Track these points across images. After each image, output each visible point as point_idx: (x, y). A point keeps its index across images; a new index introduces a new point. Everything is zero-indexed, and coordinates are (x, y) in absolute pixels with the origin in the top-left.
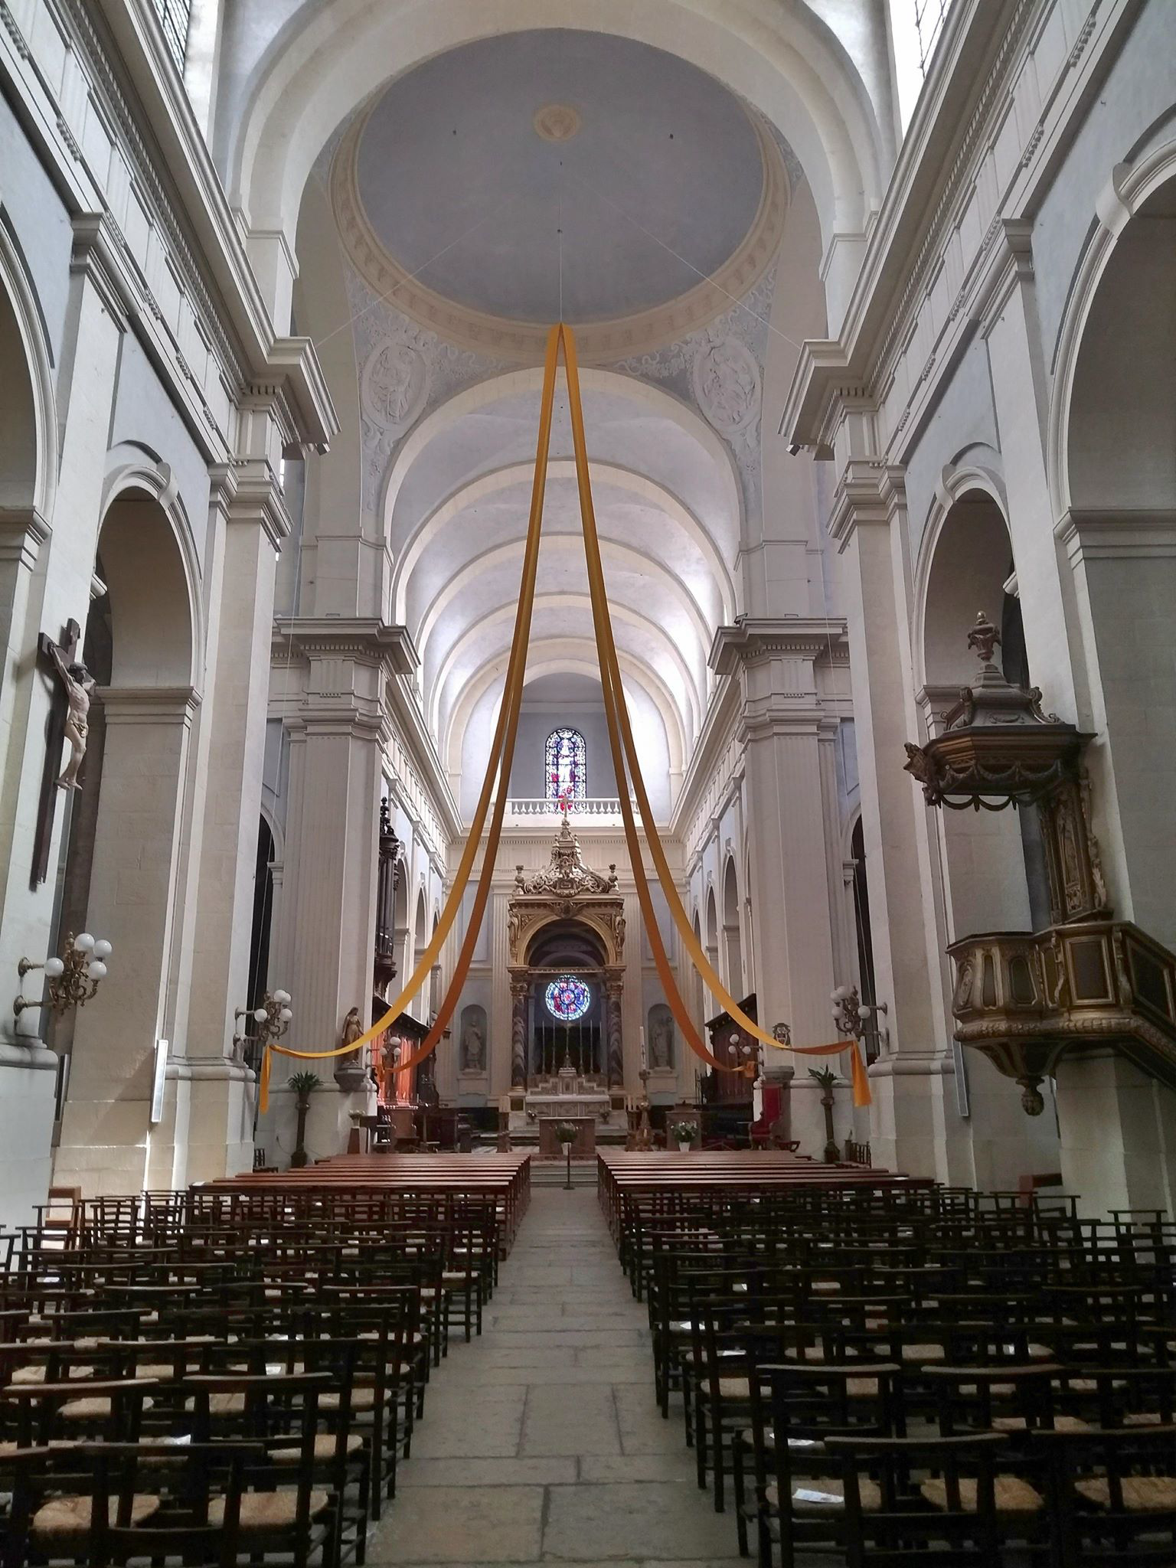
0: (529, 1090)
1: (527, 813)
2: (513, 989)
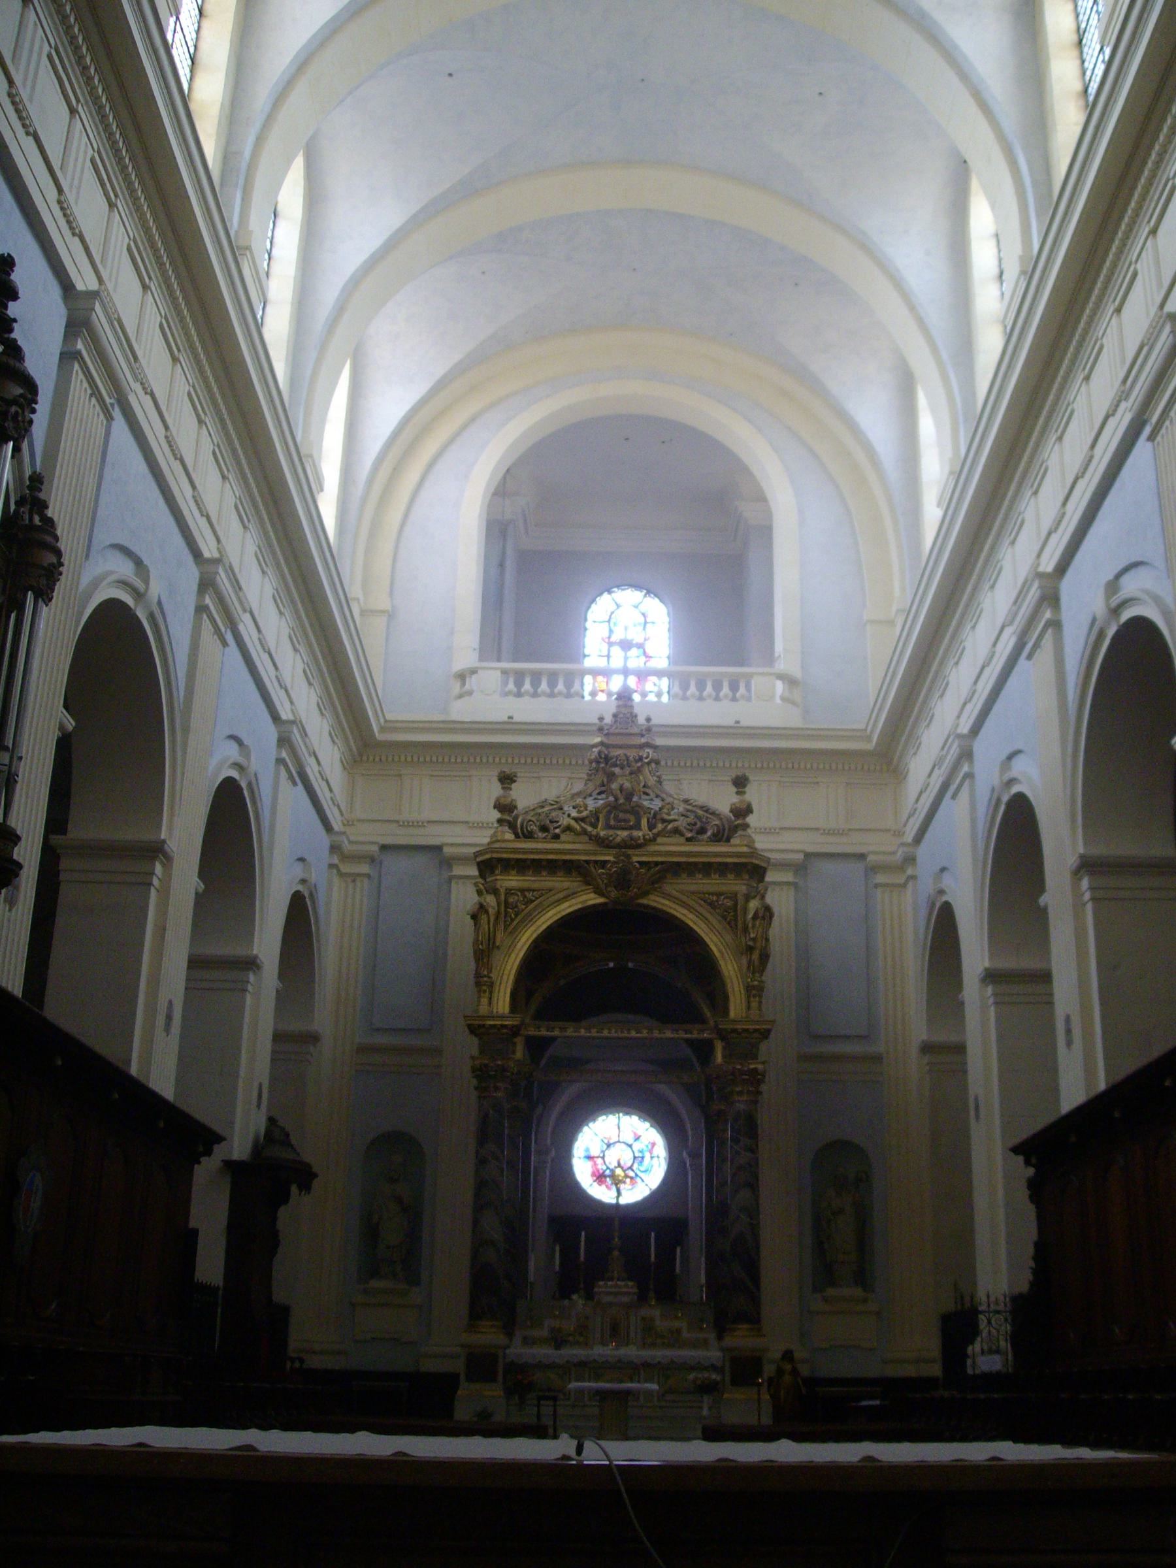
1: (535, 695)
2: (481, 1073)
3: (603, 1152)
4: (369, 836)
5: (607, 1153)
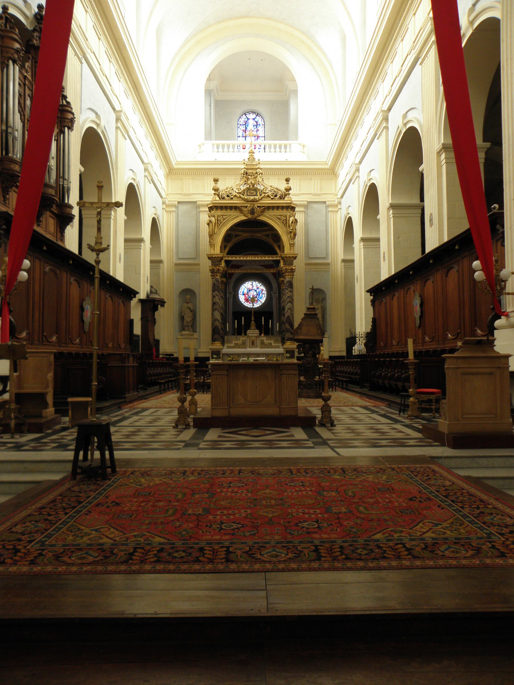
0: (226, 345)
2: (212, 271)
4: (174, 199)
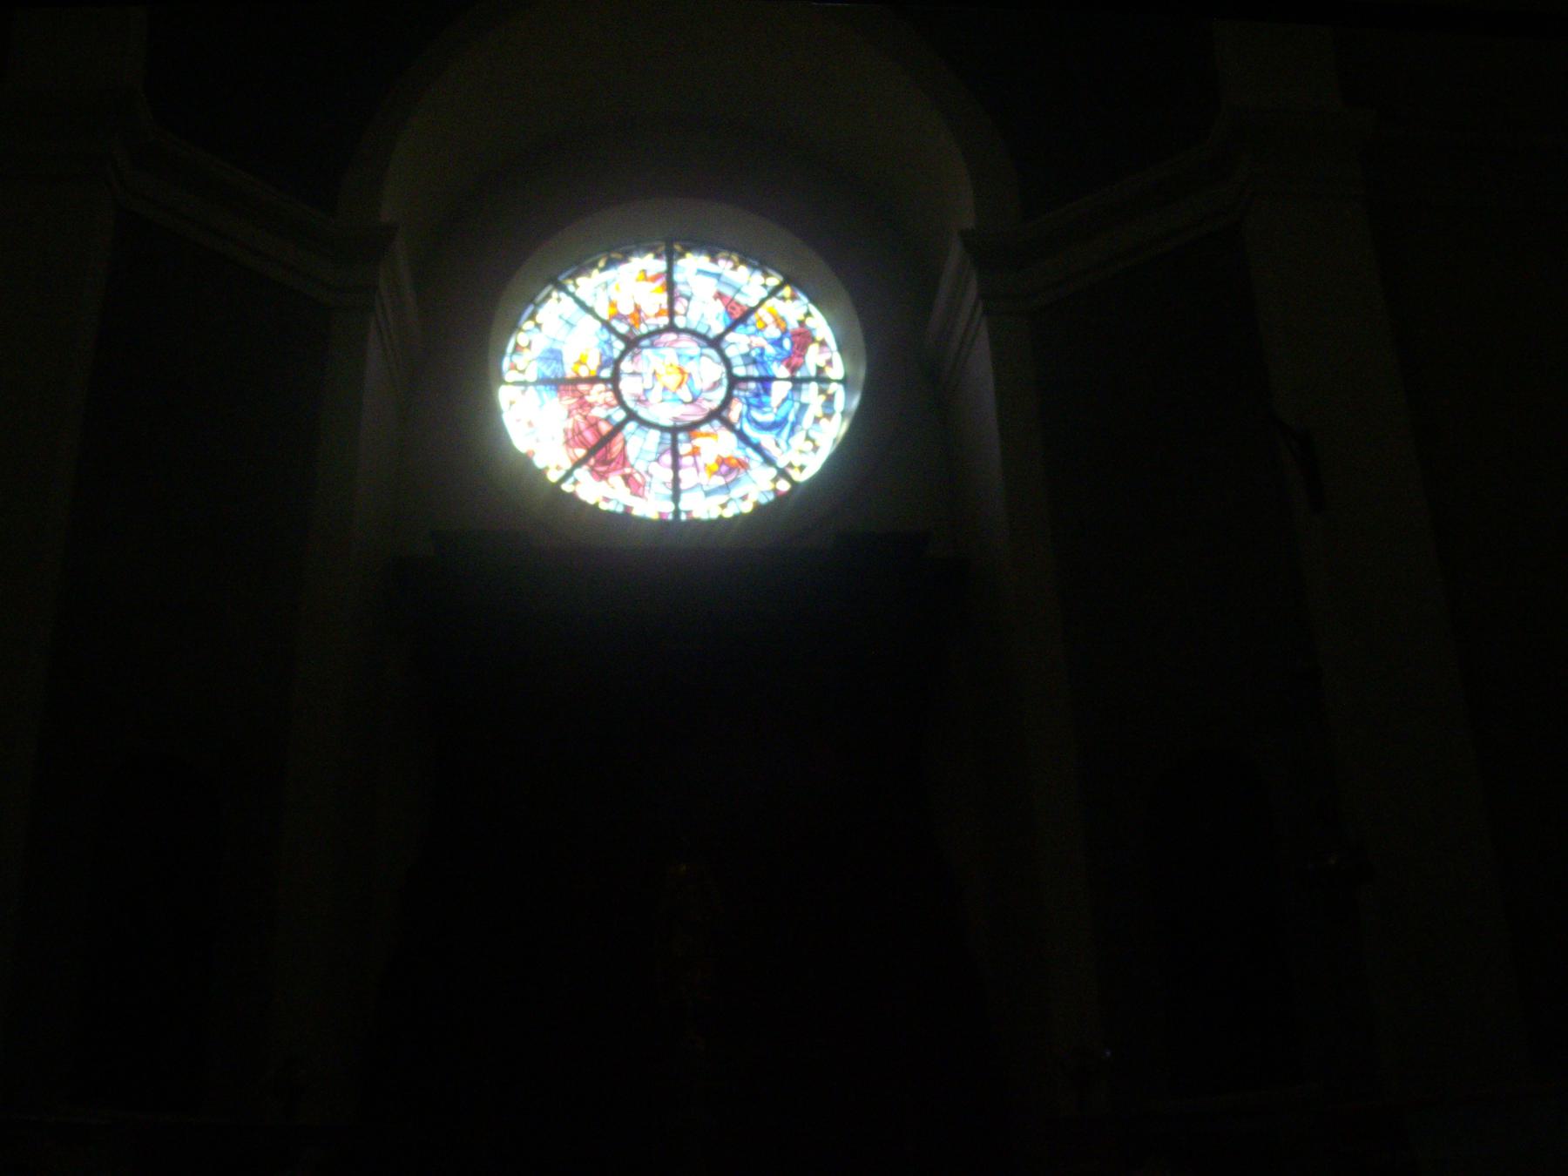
3: (616, 363)
5: (626, 366)
